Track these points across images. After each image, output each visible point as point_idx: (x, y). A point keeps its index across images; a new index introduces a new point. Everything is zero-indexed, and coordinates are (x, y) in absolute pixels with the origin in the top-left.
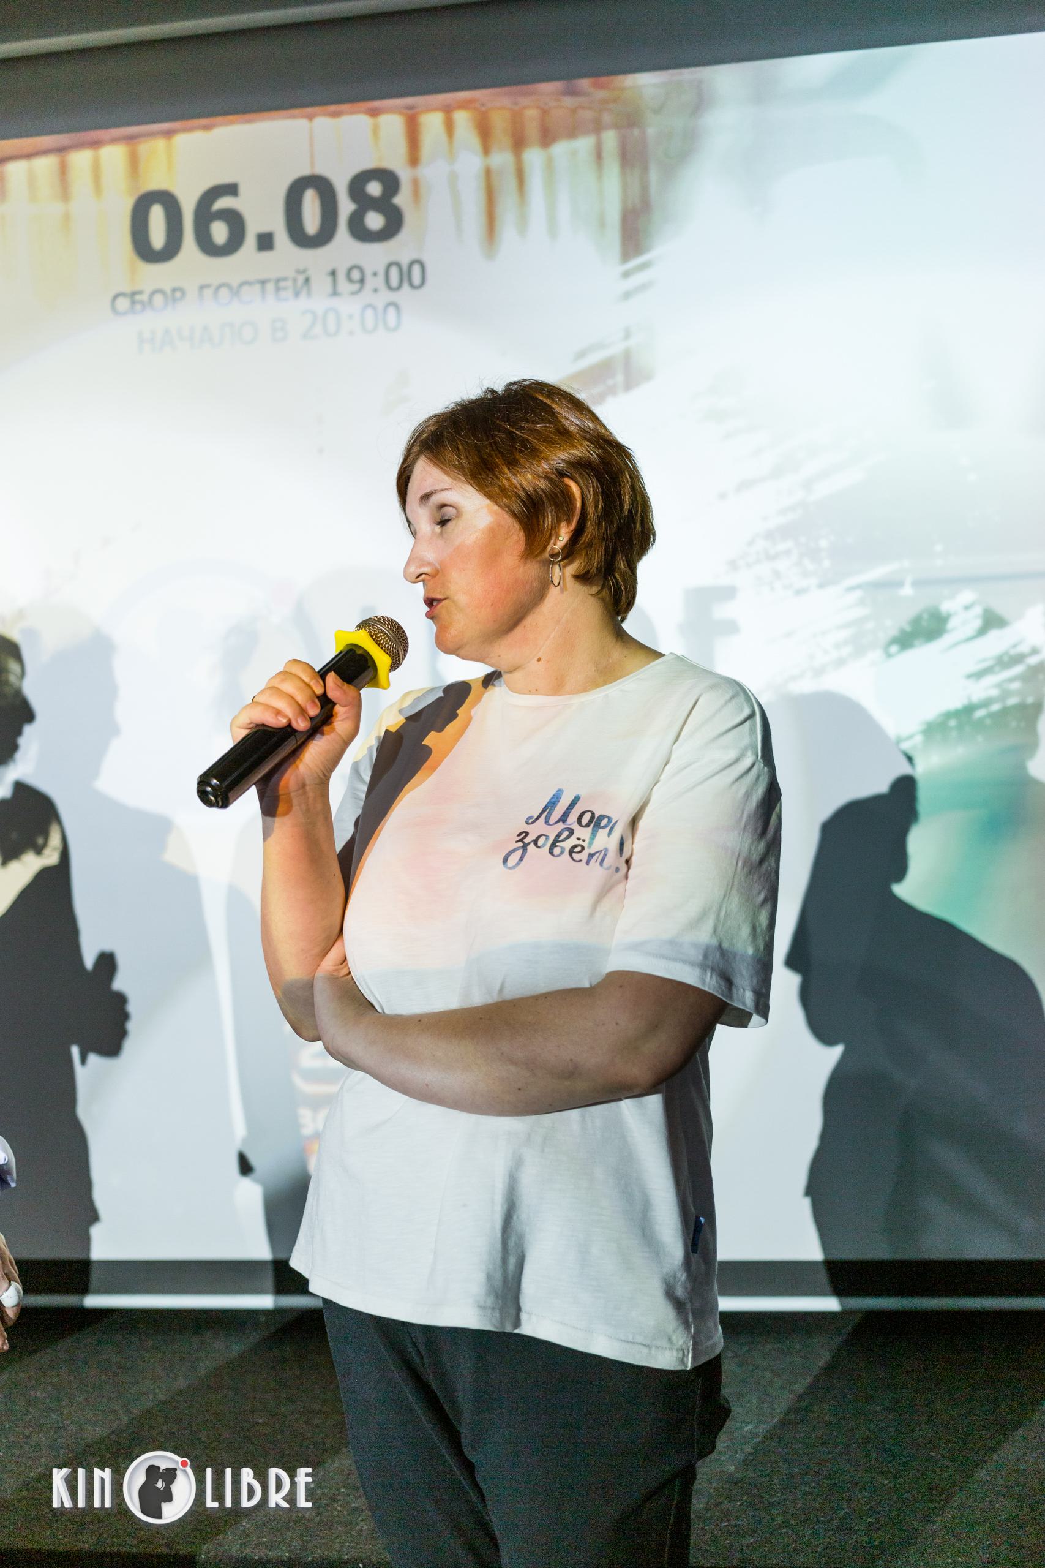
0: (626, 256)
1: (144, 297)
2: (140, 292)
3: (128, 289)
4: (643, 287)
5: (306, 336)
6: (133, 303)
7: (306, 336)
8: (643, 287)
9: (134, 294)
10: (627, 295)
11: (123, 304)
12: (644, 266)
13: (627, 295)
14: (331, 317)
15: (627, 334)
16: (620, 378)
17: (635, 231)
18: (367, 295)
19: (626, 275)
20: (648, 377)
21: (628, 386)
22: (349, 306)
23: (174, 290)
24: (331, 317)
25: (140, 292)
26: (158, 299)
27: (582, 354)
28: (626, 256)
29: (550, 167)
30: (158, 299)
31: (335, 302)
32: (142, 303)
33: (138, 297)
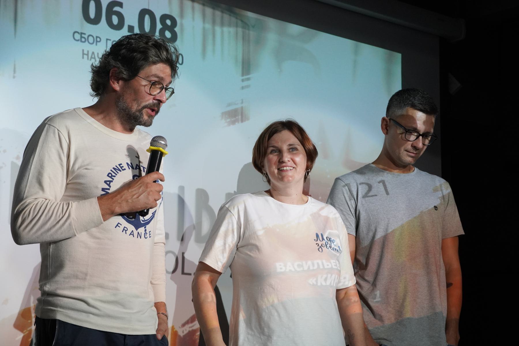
0: (243, 75)
1: (86, 36)
2: (85, 34)
3: (80, 32)
6: (81, 37)
8: (248, 86)
9: (82, 33)
10: (243, 88)
11: (77, 36)
12: (248, 79)
13: (243, 88)
15: (242, 103)
16: (240, 117)
17: (247, 67)
19: (243, 80)
20: (248, 119)
21: (242, 121)
23: (97, 37)
25: (85, 34)
26: (91, 39)
27: (229, 105)
28: (243, 75)
29: (222, 33)
30: (91, 39)
32: (84, 38)
33: (83, 36)
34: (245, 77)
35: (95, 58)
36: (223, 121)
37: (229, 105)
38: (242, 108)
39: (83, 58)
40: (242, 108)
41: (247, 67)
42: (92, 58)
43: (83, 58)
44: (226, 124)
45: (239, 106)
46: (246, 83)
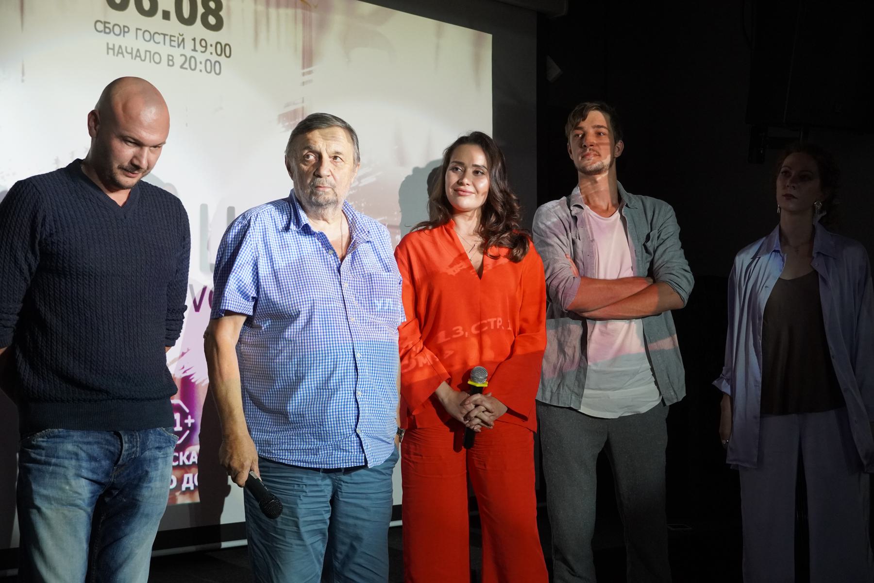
0: (304, 68)
4: (310, 81)
5: (182, 67)
7: (182, 67)
8: (310, 81)
10: (303, 83)
12: (310, 73)
13: (303, 83)
14: (193, 60)
17: (308, 57)
18: (207, 55)
19: (304, 74)
22: (200, 57)
24: (193, 60)
27: (288, 105)
28: (304, 68)
31: (194, 54)
34: (306, 70)
35: (122, 53)
36: (281, 125)
37: (288, 105)
38: (303, 108)
39: (108, 53)
40: (303, 108)
41: (308, 57)
42: (118, 53)
43: (108, 53)
44: (284, 129)
45: (299, 106)
46: (307, 77)
